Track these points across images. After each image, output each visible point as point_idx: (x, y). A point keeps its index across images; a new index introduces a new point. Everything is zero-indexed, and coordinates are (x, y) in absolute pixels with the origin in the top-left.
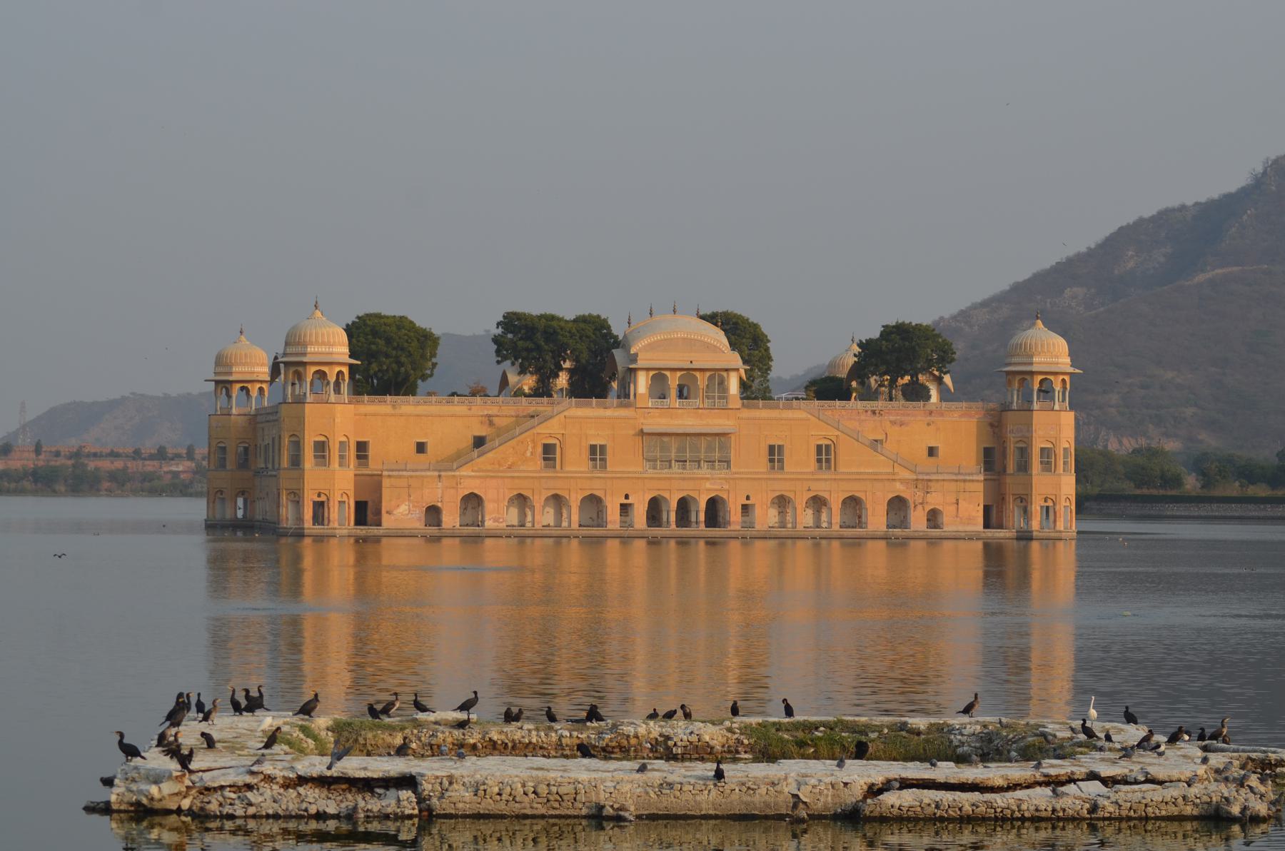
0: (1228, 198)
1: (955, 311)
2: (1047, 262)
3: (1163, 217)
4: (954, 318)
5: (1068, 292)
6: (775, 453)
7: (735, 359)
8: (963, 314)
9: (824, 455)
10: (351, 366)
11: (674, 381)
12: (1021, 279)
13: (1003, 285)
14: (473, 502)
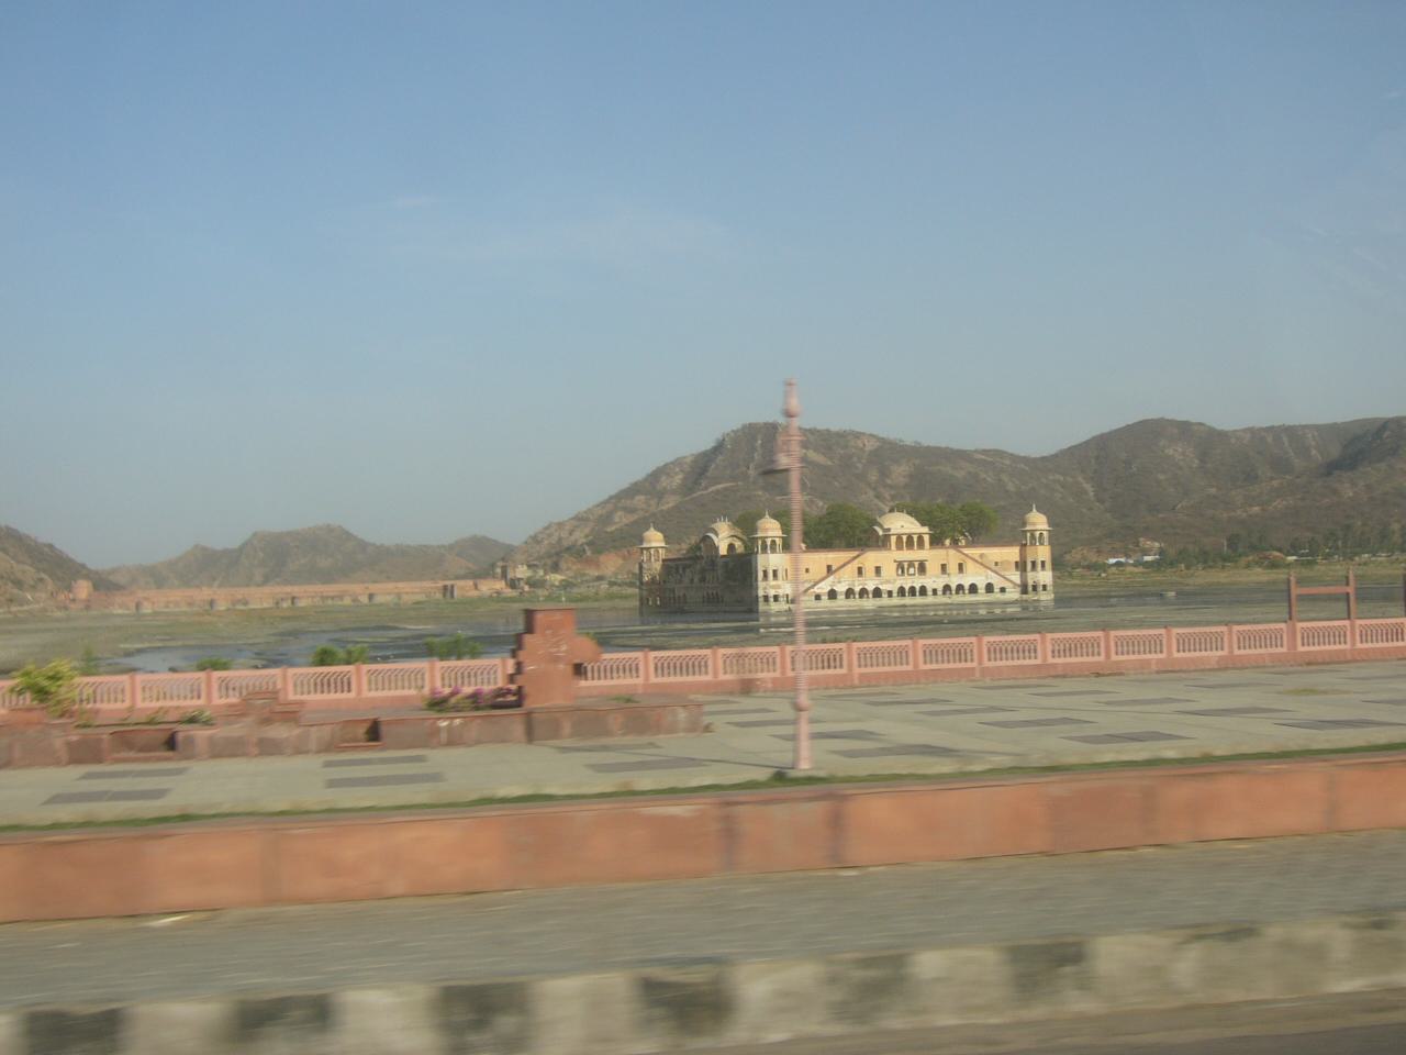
0: (704, 454)
1: (585, 509)
2: (624, 484)
3: (678, 462)
4: (585, 512)
5: (637, 498)
6: (944, 567)
7: (925, 529)
8: (589, 511)
12: (613, 493)
13: (606, 497)
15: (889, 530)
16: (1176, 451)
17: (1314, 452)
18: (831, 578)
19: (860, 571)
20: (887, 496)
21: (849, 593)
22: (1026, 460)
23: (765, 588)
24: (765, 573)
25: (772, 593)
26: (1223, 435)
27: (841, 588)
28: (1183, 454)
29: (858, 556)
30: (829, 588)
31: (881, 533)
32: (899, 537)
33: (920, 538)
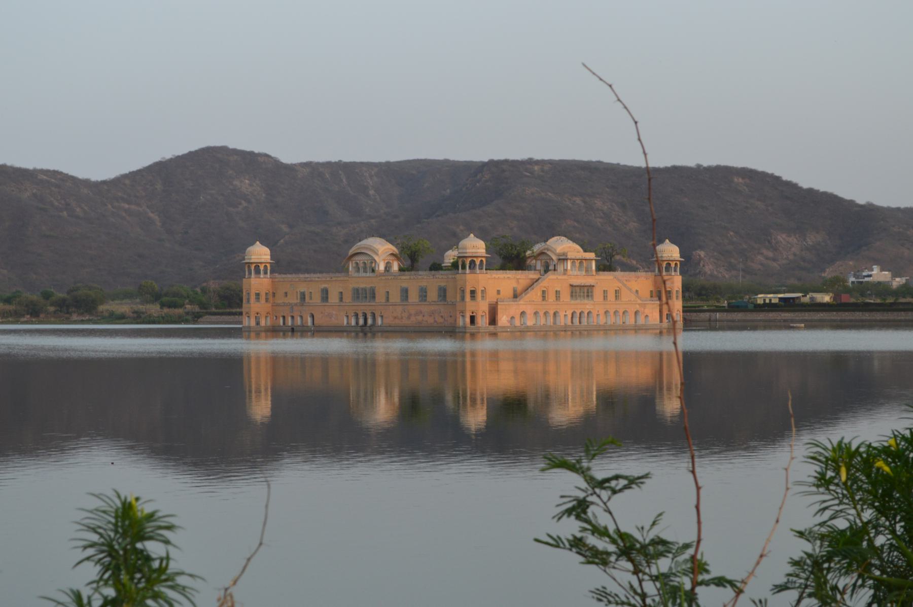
7: (592, 255)
9: (617, 293)
10: (486, 257)
11: (577, 263)
14: (523, 314)
15: (564, 254)
16: (245, 185)
17: (372, 192)
22: (87, 183)
24: (473, 293)
26: (290, 169)
28: (251, 185)
31: (554, 258)
32: (573, 260)
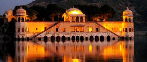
5: (42, 3)
7: (84, 15)
18: (45, 32)
19: (57, 30)
20: (129, 4)
21: (53, 39)
23: (19, 35)
24: (19, 29)
25: (21, 37)
27: (49, 36)
29: (57, 24)
30: (44, 36)
33: (82, 18)
